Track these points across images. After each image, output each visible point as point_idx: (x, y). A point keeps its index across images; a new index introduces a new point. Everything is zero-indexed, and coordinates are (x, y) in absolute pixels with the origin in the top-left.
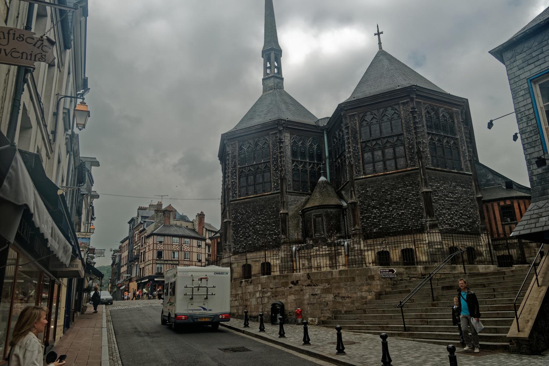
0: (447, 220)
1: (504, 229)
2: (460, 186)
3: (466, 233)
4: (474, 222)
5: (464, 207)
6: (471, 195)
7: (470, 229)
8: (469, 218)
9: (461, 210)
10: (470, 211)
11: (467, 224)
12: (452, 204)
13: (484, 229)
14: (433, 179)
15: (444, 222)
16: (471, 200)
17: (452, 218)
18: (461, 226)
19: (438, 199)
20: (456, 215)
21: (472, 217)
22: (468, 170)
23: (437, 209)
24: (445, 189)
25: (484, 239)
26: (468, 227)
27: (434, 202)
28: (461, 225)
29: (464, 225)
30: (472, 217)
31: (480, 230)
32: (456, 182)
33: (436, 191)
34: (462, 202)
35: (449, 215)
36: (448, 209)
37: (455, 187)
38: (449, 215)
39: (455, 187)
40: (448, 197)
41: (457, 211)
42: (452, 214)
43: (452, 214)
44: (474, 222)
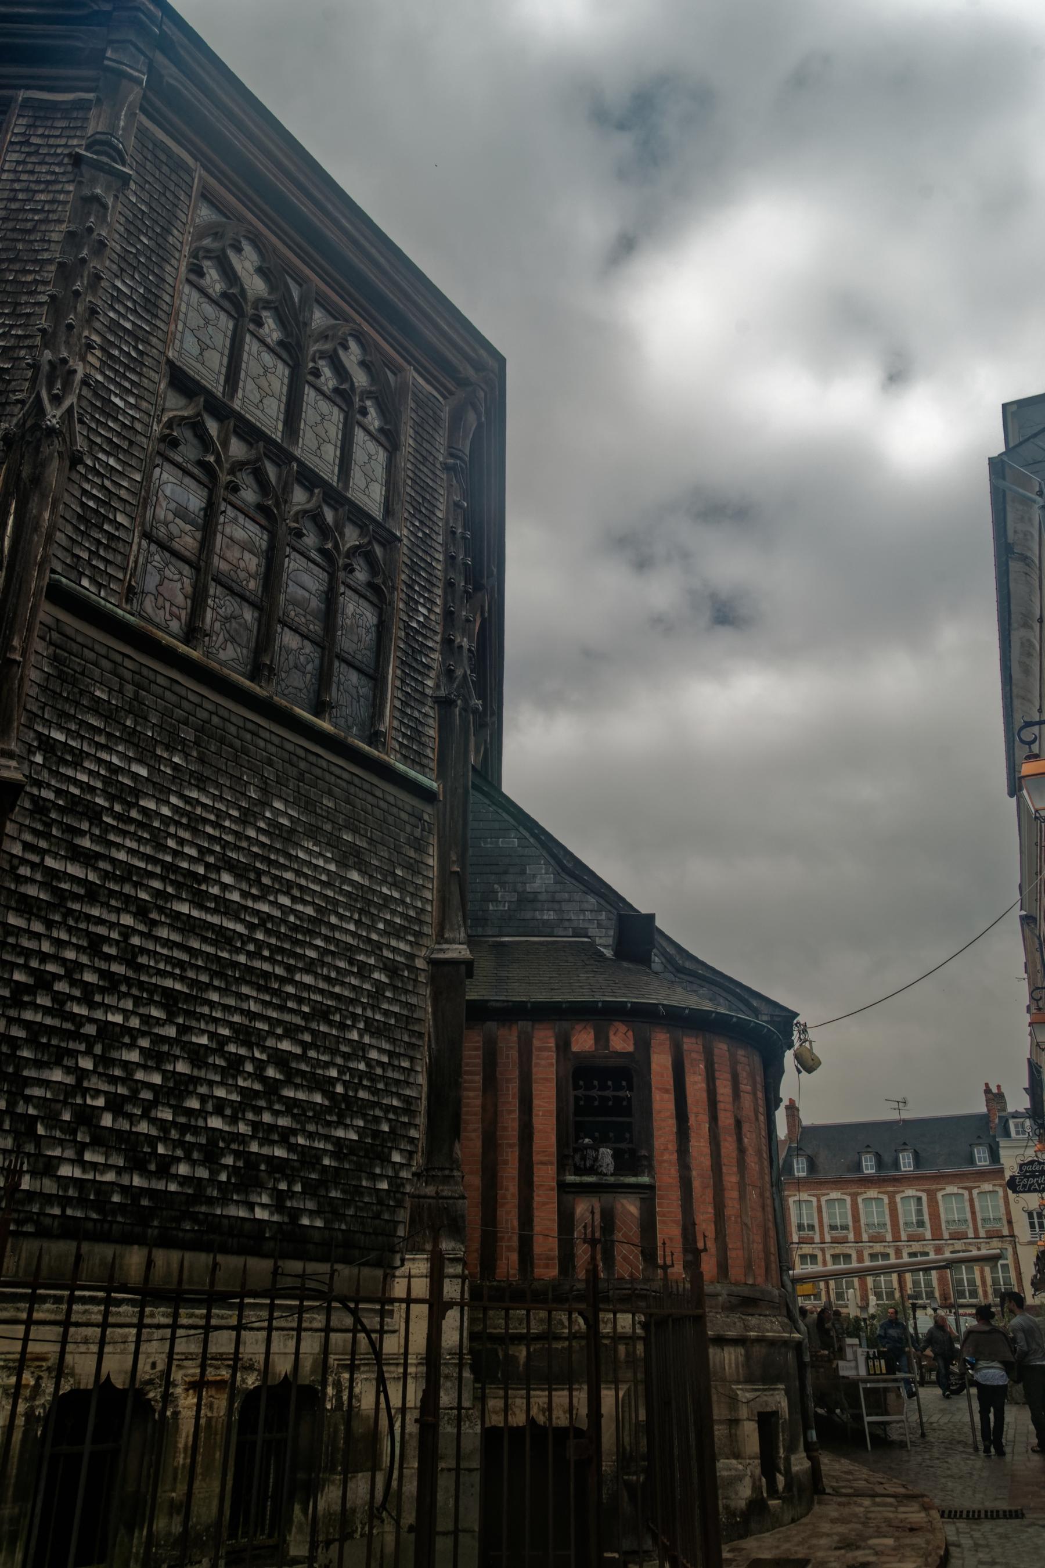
0: (115, 1105)
1: (566, 1220)
2: (334, 842)
3: (290, 1240)
4: (372, 1151)
5: (322, 1014)
6: (397, 932)
7: (329, 1210)
8: (343, 1108)
9: (291, 1032)
10: (359, 1050)
11: (309, 1158)
12: (219, 968)
13: (436, 1222)
14: (96, 707)
15: (86, 1117)
16: (392, 969)
17: (177, 1089)
18: (249, 1176)
19: (92, 894)
20: (235, 1064)
21: (362, 1108)
22: (417, 761)
23: (43, 981)
24: (194, 824)
25: (417, 1307)
26: (311, 1190)
27: (27, 907)
28: (251, 1161)
29: (277, 1166)
30: (362, 1108)
31: (403, 1215)
32: (308, 805)
33: (94, 815)
34: (310, 967)
35: (155, 1058)
36: (170, 1000)
37: (288, 836)
38: (155, 1058)
39: (288, 836)
40: (199, 899)
41: (245, 1035)
42: (197, 1056)
43: (197, 1056)
44: (372, 1151)
